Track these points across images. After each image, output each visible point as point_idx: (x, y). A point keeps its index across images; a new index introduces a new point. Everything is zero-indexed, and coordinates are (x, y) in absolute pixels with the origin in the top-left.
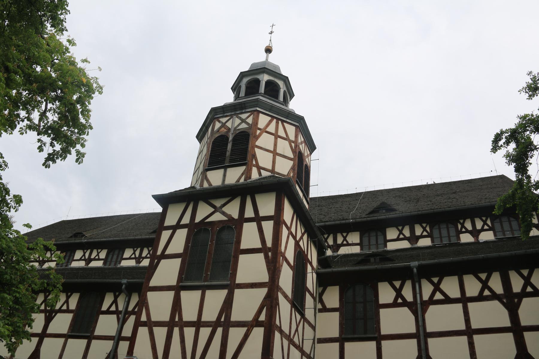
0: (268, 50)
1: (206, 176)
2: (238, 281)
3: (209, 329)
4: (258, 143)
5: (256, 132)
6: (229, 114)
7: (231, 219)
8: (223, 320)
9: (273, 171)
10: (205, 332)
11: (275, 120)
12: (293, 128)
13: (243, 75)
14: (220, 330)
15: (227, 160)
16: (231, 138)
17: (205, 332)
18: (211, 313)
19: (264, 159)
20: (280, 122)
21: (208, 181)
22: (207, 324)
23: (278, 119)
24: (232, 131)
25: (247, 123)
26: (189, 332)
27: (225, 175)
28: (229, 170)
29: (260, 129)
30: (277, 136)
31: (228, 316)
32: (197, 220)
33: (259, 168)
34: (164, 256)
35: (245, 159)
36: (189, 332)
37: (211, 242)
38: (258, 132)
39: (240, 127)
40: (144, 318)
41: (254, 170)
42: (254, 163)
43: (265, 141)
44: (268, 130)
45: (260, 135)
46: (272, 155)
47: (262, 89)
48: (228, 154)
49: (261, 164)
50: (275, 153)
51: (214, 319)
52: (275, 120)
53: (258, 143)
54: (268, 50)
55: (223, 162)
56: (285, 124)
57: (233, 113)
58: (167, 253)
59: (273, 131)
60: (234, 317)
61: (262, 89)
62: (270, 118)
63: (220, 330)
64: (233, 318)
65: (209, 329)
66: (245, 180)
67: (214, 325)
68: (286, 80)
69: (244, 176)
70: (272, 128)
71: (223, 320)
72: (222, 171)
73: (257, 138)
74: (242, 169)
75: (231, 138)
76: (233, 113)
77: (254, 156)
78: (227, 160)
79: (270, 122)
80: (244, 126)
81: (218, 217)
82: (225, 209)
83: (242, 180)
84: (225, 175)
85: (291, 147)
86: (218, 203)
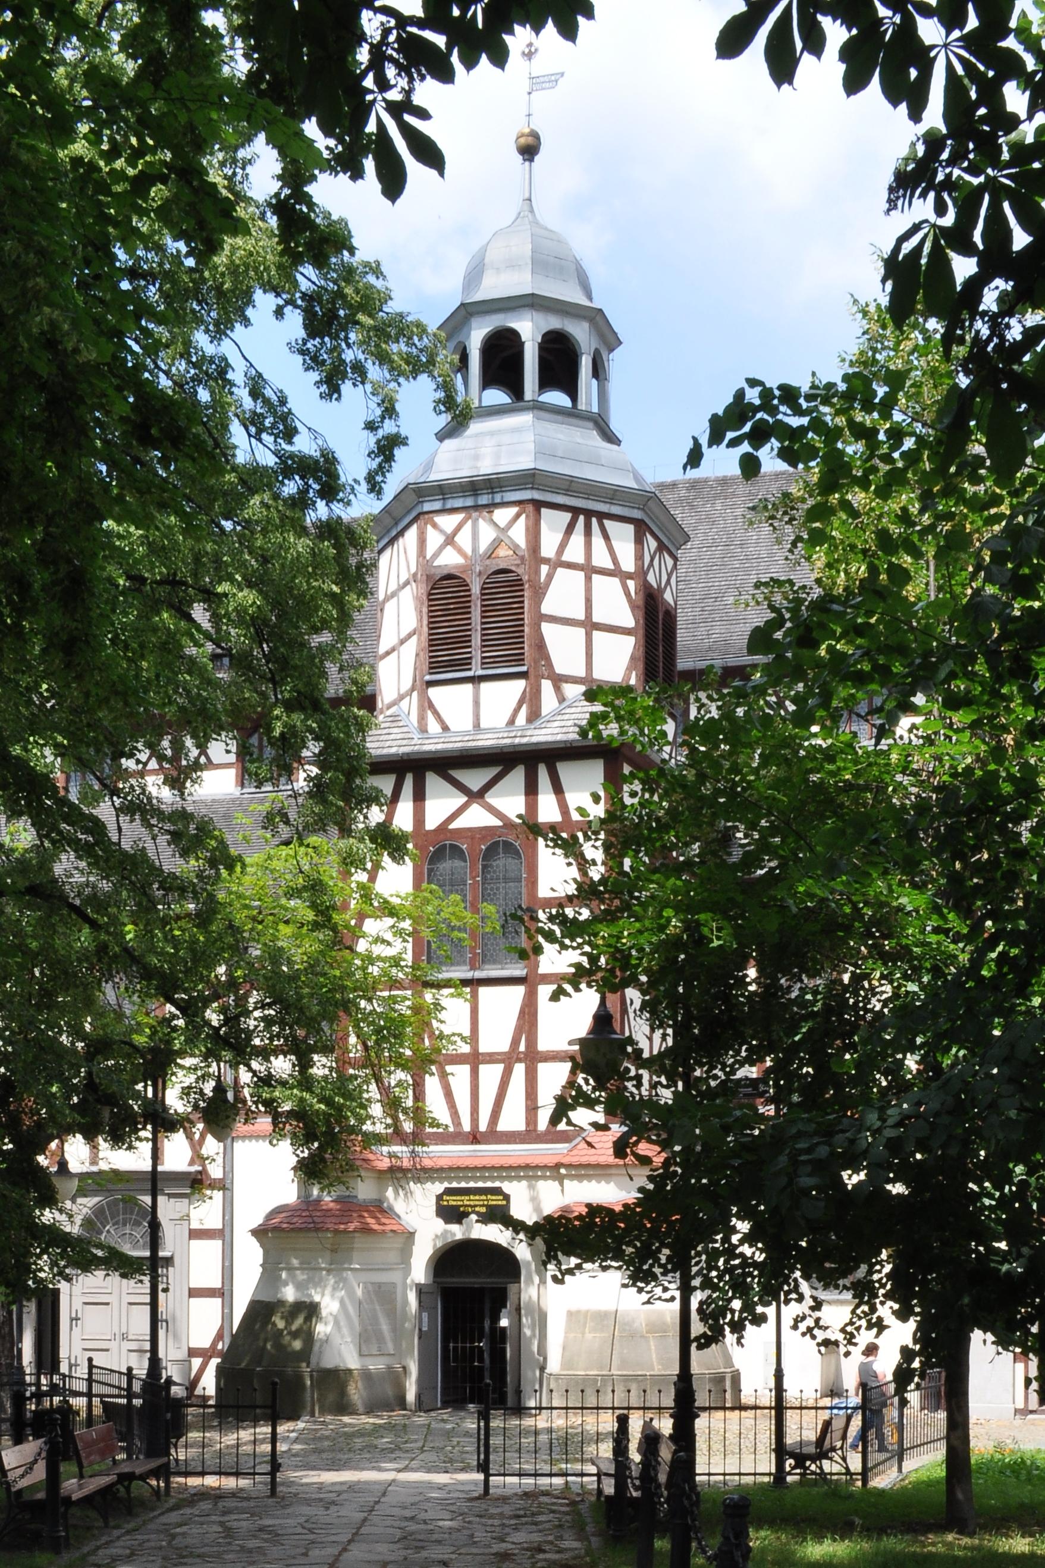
0: (529, 150)
1: (431, 706)
2: (541, 971)
3: (499, 1068)
4: (546, 608)
5: (538, 572)
6: (458, 503)
7: (508, 824)
8: (522, 1048)
10: (491, 1074)
11: (582, 518)
12: (630, 528)
14: (519, 1069)
15: (477, 656)
16: (476, 589)
17: (491, 1074)
18: (497, 1036)
19: (564, 648)
20: (594, 520)
21: (436, 713)
22: (492, 1058)
23: (589, 514)
26: (460, 1075)
27: (477, 703)
28: (485, 686)
29: (547, 561)
30: (589, 570)
31: (532, 1042)
32: (431, 823)
33: (558, 680)
35: (519, 660)
36: (460, 1075)
37: (473, 878)
38: (544, 569)
41: (547, 686)
43: (563, 595)
44: (566, 557)
45: (550, 577)
46: (582, 631)
48: (476, 640)
49: (560, 669)
50: (590, 626)
51: (504, 1046)
52: (582, 518)
53: (546, 608)
54: (529, 150)
55: (465, 663)
56: (606, 522)
57: (469, 502)
59: (580, 559)
60: (543, 1045)
62: (567, 516)
63: (519, 1069)
64: (543, 1045)
65: (499, 1068)
67: (508, 1060)
68: (596, 318)
69: (524, 708)
70: (575, 551)
71: (522, 1048)
72: (468, 687)
73: (540, 592)
74: (518, 686)
75: (476, 589)
76: (469, 502)
77: (541, 646)
78: (477, 656)
79: (570, 529)
81: (476, 817)
82: (491, 798)
83: (521, 719)
84: (477, 703)
85: (627, 593)
86: (475, 779)
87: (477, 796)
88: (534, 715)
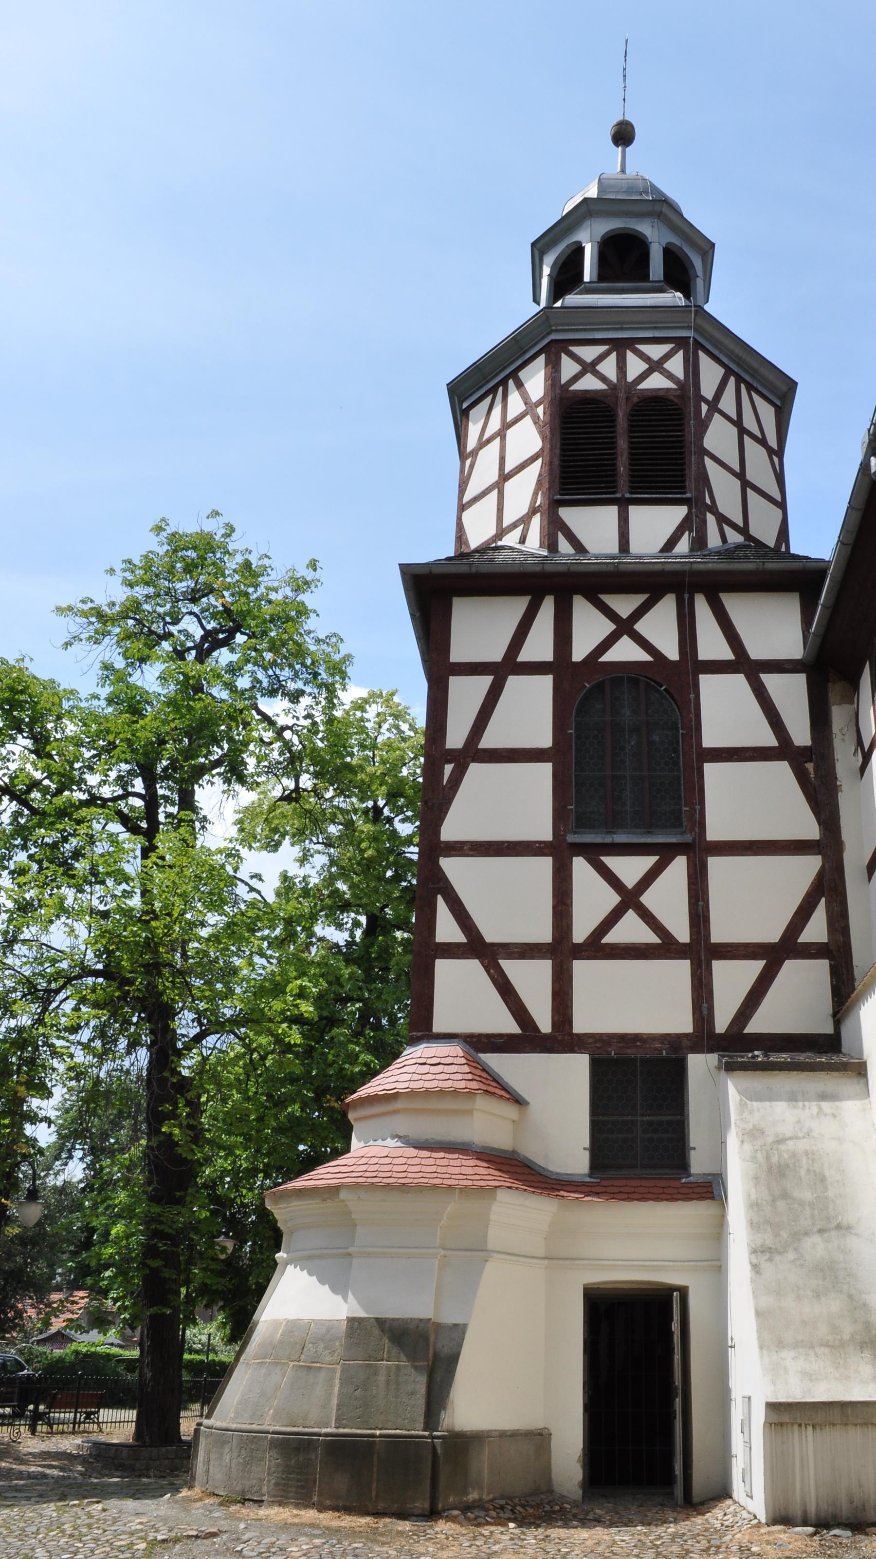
9: (744, 530)
13: (586, 210)
16: (621, 414)
24: (622, 395)
25: (670, 376)
28: (636, 513)
34: (473, 752)
38: (704, 408)
39: (644, 385)
40: (447, 930)
42: (708, 501)
43: (719, 438)
47: (656, 268)
58: (487, 742)
61: (656, 268)
66: (692, 550)
73: (703, 426)
75: (621, 414)
77: (704, 480)
80: (656, 382)
83: (683, 546)
86: (624, 605)
87: (625, 627)
88: (699, 543)
